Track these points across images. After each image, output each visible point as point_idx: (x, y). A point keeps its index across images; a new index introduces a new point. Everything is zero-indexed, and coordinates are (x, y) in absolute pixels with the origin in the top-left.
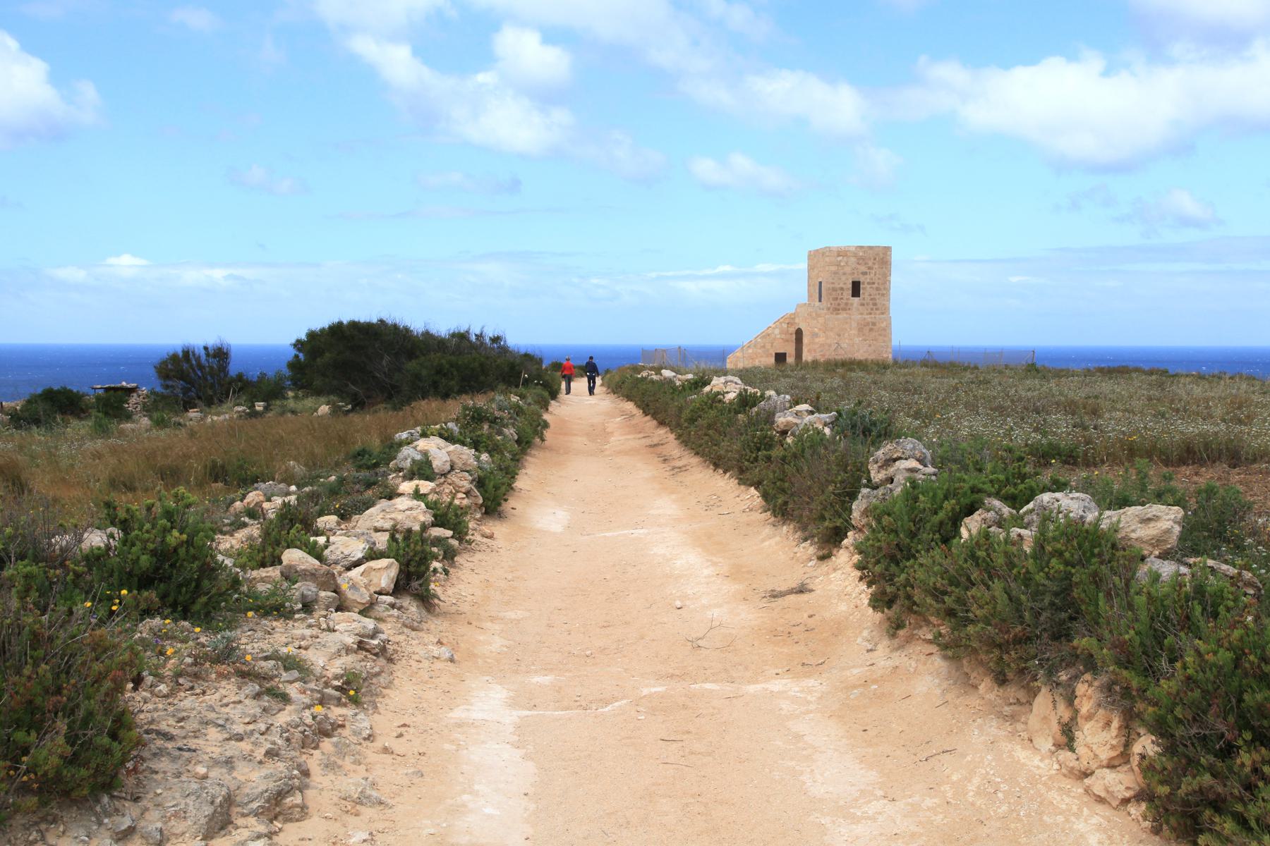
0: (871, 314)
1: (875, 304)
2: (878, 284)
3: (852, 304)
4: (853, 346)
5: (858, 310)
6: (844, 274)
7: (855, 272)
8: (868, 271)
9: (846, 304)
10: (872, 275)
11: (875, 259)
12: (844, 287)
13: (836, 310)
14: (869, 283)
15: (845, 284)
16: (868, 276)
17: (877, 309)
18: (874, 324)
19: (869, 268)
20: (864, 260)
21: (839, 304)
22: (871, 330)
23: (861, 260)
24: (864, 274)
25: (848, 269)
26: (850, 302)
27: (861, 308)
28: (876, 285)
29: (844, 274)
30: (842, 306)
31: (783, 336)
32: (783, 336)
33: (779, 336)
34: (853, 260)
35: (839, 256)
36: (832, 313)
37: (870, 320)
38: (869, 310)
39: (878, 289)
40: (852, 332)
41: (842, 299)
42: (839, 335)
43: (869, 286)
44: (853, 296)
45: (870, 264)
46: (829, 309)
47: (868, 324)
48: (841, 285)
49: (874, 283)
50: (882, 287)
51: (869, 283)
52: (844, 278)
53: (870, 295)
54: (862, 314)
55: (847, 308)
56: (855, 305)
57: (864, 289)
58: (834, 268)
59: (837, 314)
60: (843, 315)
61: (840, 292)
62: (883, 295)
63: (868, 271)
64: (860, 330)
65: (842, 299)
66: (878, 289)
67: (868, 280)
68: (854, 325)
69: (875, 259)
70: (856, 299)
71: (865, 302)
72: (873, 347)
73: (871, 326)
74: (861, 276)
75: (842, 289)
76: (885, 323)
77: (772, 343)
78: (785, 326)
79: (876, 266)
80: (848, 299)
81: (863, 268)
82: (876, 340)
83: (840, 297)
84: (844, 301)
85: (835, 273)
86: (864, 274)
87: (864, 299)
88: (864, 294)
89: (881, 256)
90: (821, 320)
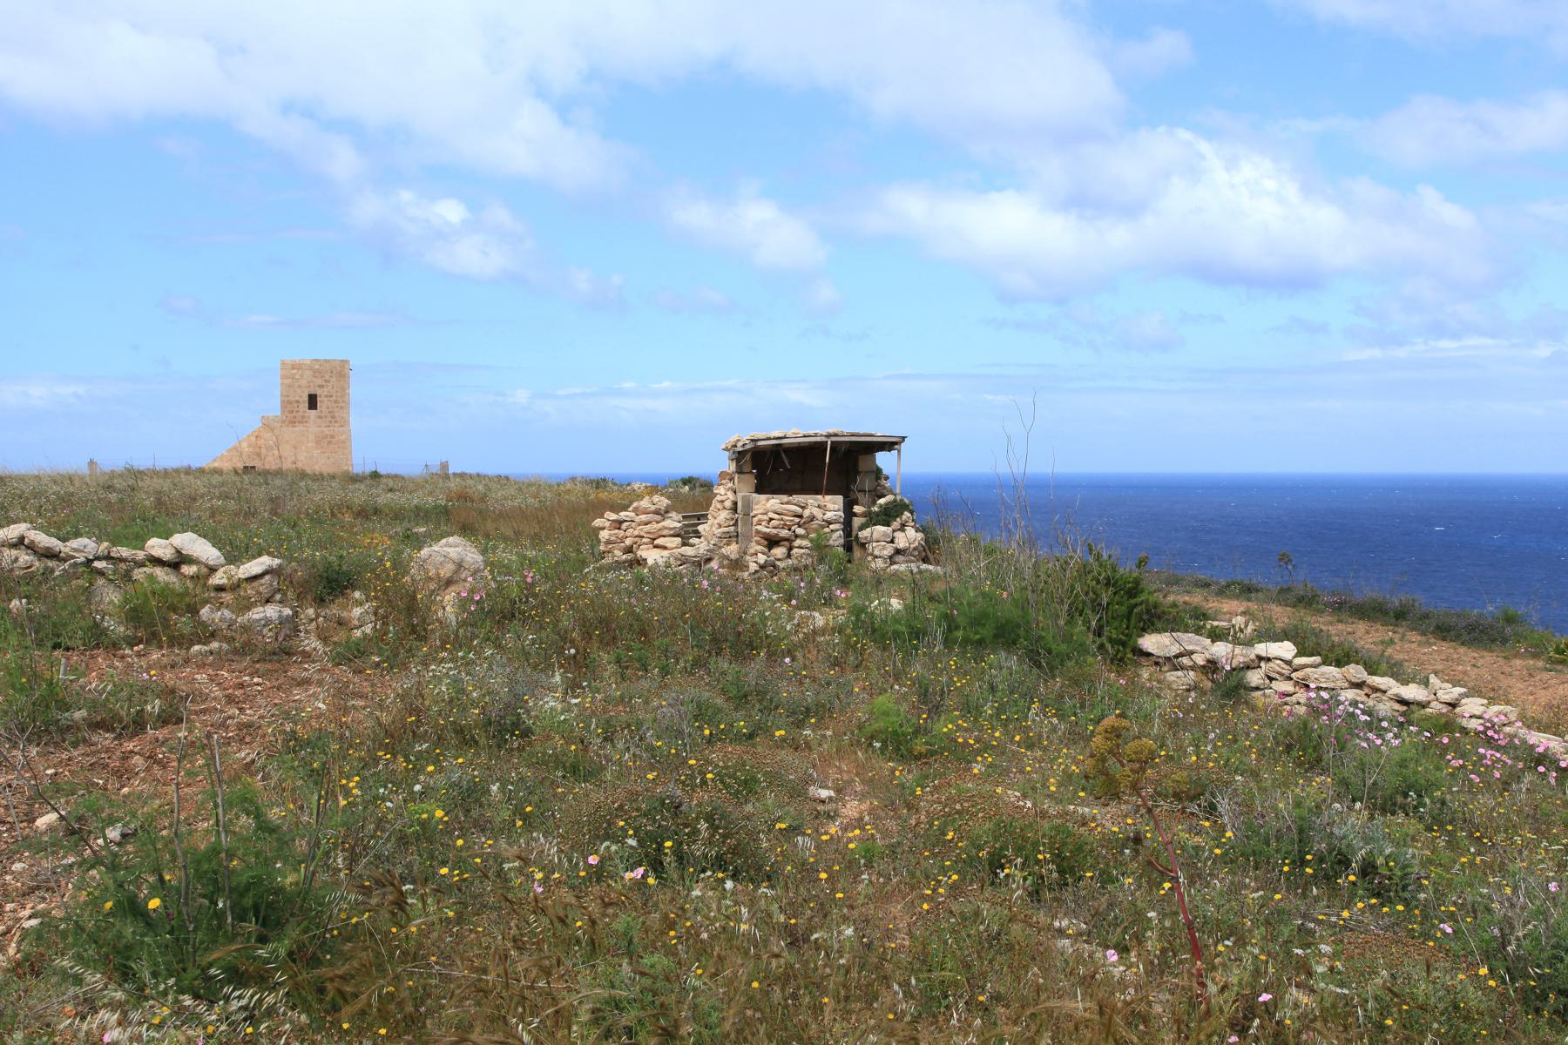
1: (333, 417)
3: (309, 417)
9: (303, 417)
12: (301, 400)
13: (293, 423)
14: (326, 396)
16: (325, 389)
17: (336, 422)
18: (332, 437)
19: (326, 381)
22: (329, 442)
23: (316, 373)
24: (321, 386)
25: (304, 382)
27: (319, 420)
28: (334, 398)
29: (300, 386)
30: (299, 419)
32: (251, 449)
34: (309, 373)
35: (293, 368)
39: (336, 402)
40: (310, 445)
42: (295, 448)
45: (327, 377)
47: (326, 437)
48: (297, 398)
50: (340, 400)
51: (326, 396)
52: (299, 391)
55: (303, 421)
56: (312, 418)
58: (288, 381)
60: (299, 428)
62: (342, 408)
64: (318, 442)
66: (336, 402)
68: (312, 437)
70: (313, 412)
72: (332, 460)
75: (298, 402)
76: (344, 436)
78: (253, 439)
80: (304, 412)
81: (320, 381)
85: (290, 386)
86: (321, 386)
89: (339, 369)
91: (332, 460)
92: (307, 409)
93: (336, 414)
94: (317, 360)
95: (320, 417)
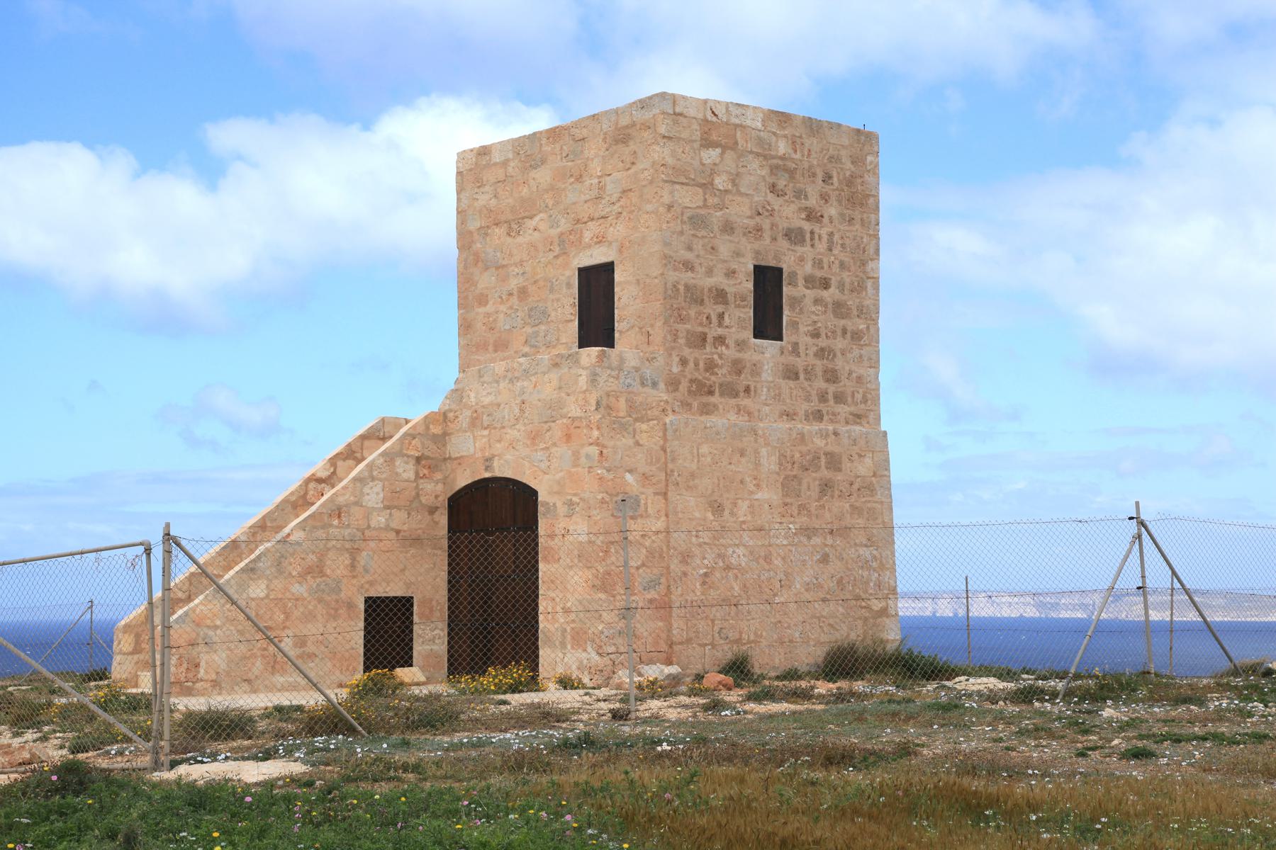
0: (819, 416)
2: (841, 286)
3: (756, 370)
4: (768, 559)
5: (778, 397)
6: (728, 228)
7: (766, 224)
8: (807, 226)
10: (821, 247)
11: (827, 178)
12: (730, 287)
14: (810, 281)
15: (731, 273)
16: (805, 250)
17: (839, 398)
18: (834, 462)
20: (792, 173)
21: (711, 367)
24: (795, 236)
25: (739, 211)
26: (747, 356)
27: (786, 385)
28: (831, 294)
29: (728, 228)
30: (723, 374)
31: (399, 519)
32: (399, 519)
33: (379, 520)
34: (756, 170)
35: (707, 144)
36: (686, 405)
37: (820, 443)
38: (815, 404)
41: (720, 340)
43: (810, 294)
44: (758, 334)
46: (673, 384)
48: (718, 280)
49: (825, 284)
50: (852, 302)
51: (810, 281)
53: (816, 335)
54: (789, 415)
57: (796, 301)
58: (689, 198)
59: (706, 410)
60: (724, 419)
61: (713, 309)
62: (857, 336)
63: (807, 226)
64: (789, 485)
65: (720, 340)
66: (839, 309)
67: (808, 268)
68: (769, 462)
69: (827, 178)
70: (769, 346)
71: (800, 363)
72: (835, 566)
73: (825, 473)
74: (783, 244)
75: (720, 296)
77: (354, 553)
78: (406, 470)
79: (832, 211)
81: (790, 215)
82: (844, 531)
83: (715, 331)
84: (730, 353)
85: (698, 221)
87: (795, 350)
88: (795, 325)
90: (648, 435)
91: (835, 566)
92: (749, 333)
93: (839, 363)
94: (783, 118)
95: (791, 374)
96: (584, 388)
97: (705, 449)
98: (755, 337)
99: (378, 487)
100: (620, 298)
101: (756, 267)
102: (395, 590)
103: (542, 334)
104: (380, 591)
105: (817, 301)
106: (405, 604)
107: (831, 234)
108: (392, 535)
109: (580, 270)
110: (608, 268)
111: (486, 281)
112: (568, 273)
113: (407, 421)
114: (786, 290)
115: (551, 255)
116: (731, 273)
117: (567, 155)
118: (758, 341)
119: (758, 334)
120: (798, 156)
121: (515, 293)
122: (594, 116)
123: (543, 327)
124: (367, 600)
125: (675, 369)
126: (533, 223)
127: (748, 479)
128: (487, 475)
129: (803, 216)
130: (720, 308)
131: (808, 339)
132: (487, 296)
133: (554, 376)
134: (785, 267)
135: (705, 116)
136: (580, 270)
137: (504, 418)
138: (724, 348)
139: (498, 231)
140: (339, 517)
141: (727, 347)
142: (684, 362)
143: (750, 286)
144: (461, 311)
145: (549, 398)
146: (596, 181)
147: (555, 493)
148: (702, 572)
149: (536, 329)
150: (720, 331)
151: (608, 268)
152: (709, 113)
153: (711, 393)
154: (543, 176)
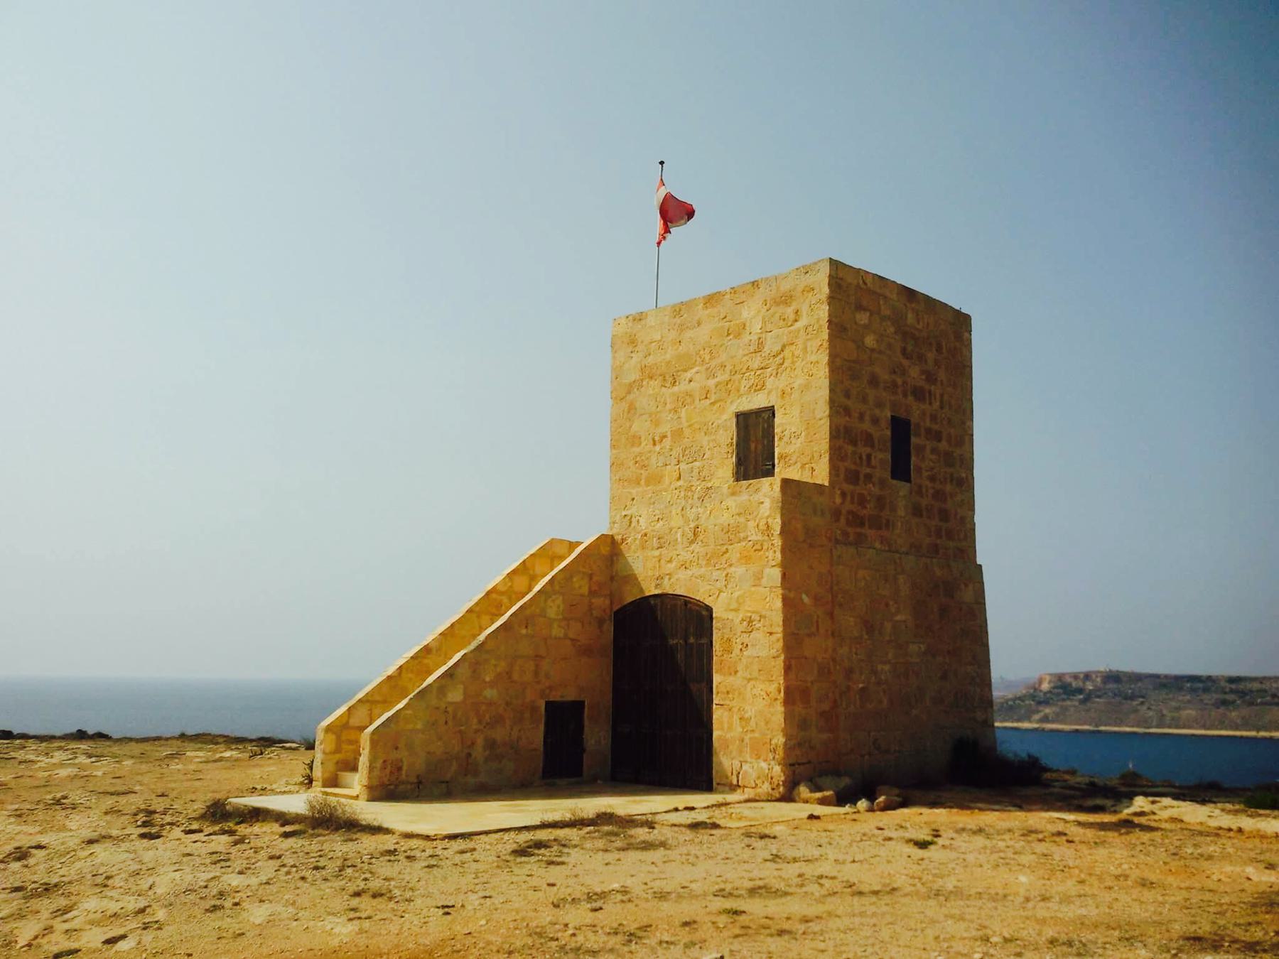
10: (936, 404)
11: (939, 350)
15: (875, 421)
28: (943, 445)
30: (869, 510)
41: (869, 477)
43: (929, 445)
44: (894, 476)
48: (867, 426)
53: (932, 479)
57: (921, 449)
65: (869, 477)
70: (903, 488)
71: (924, 502)
75: (869, 439)
87: (920, 493)
88: (919, 470)
92: (887, 475)
96: (766, 514)
97: (861, 573)
98: (893, 477)
99: (559, 601)
100: (780, 439)
101: (892, 416)
102: (570, 695)
103: (696, 471)
104: (556, 696)
105: (934, 451)
106: (577, 706)
107: (942, 396)
108: (569, 642)
109: (738, 415)
110: (771, 411)
111: (640, 426)
112: (725, 417)
113: (572, 545)
114: (914, 440)
115: (708, 402)
116: (875, 421)
117: (725, 317)
118: (895, 482)
119: (894, 476)
120: (920, 327)
121: (669, 434)
122: (753, 283)
123: (697, 464)
124: (547, 703)
125: (838, 500)
126: (689, 375)
127: (891, 603)
128: (657, 592)
129: (924, 377)
130: (868, 450)
131: (928, 483)
132: (640, 438)
133: (731, 502)
134: (913, 421)
135: (858, 283)
136: (738, 415)
137: (677, 539)
138: (871, 485)
139: (655, 383)
140: (526, 627)
141: (874, 485)
142: (843, 495)
143: (889, 433)
144: (614, 451)
145: (726, 524)
146: (756, 337)
147: (732, 610)
148: (861, 686)
149: (690, 465)
150: (868, 470)
151: (771, 411)
152: (861, 282)
153: (862, 524)
154: (703, 334)
